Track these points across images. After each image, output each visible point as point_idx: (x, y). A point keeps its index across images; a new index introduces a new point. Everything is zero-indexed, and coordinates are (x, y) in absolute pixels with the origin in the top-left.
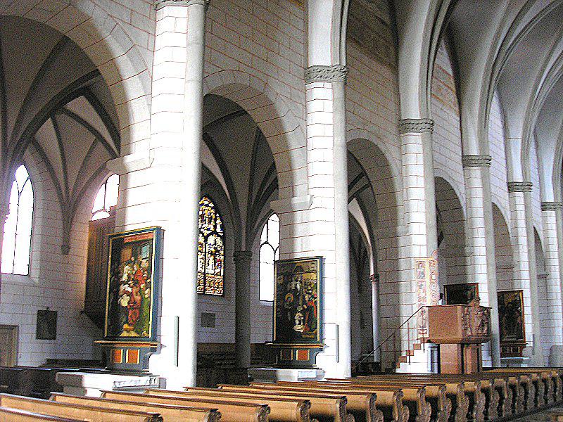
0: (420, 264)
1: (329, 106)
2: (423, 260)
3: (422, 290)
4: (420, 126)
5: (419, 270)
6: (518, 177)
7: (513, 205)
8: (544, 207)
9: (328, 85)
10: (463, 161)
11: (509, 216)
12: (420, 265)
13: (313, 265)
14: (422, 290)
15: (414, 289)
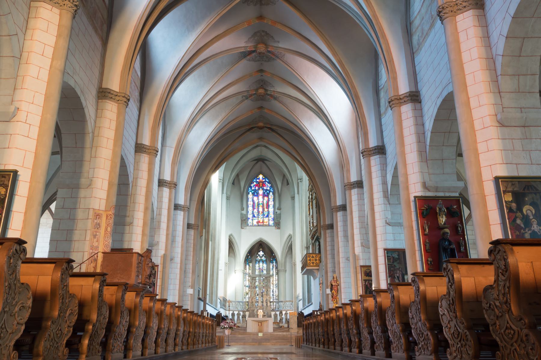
0: (98, 216)
1: (54, 29)
2: (101, 212)
3: (95, 240)
4: (117, 98)
5: (96, 221)
6: (167, 177)
7: (160, 198)
8: (177, 207)
9: (56, 11)
10: (136, 147)
11: (156, 206)
12: (98, 217)
13: (3, 179)
14: (95, 240)
15: (88, 238)
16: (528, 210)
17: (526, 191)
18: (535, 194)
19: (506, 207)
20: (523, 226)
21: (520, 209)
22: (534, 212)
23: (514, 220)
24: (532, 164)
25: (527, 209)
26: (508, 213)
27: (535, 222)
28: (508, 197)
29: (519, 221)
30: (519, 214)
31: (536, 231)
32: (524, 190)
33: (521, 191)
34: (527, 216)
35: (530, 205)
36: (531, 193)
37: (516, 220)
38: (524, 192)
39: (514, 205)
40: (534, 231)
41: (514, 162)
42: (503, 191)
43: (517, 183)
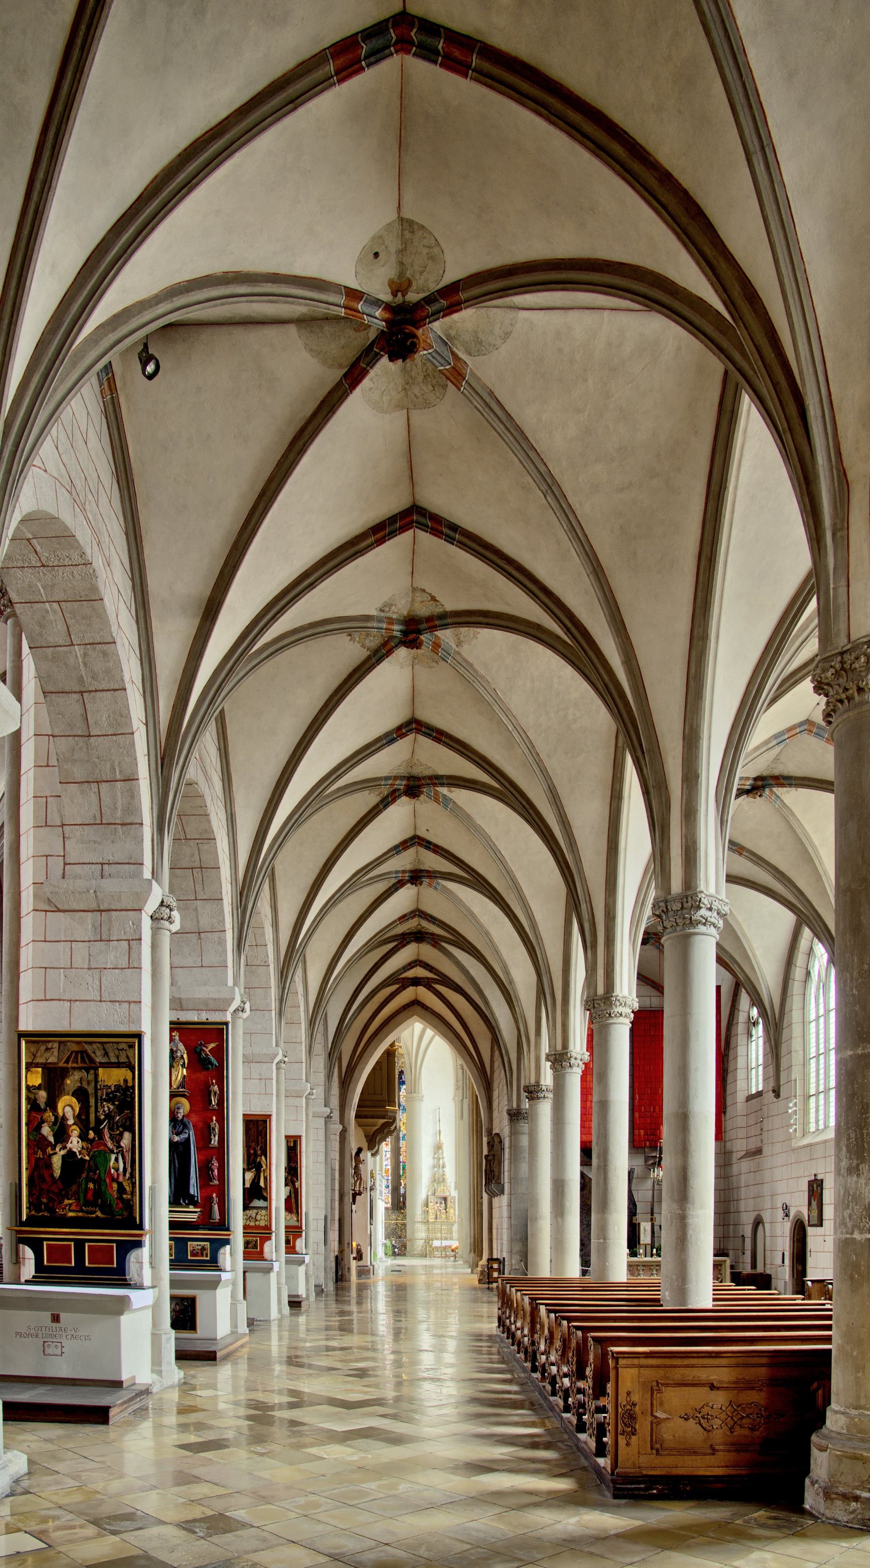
16: (69, 1105)
17: (70, 1065)
18: (87, 1070)
19: (28, 1098)
20: (51, 1139)
21: (52, 1104)
22: (77, 1110)
23: (39, 1127)
24: (101, 1001)
25: (68, 1106)
26: (29, 1112)
27: (75, 1132)
28: (36, 1078)
29: (46, 1130)
30: (49, 1115)
31: (75, 1150)
32: (67, 1062)
33: (61, 1064)
34: (64, 1118)
35: (75, 1094)
36: (80, 1069)
37: (41, 1127)
38: (65, 1065)
39: (43, 1095)
40: (71, 1153)
41: (67, 997)
42: (27, 1064)
43: (56, 1045)
